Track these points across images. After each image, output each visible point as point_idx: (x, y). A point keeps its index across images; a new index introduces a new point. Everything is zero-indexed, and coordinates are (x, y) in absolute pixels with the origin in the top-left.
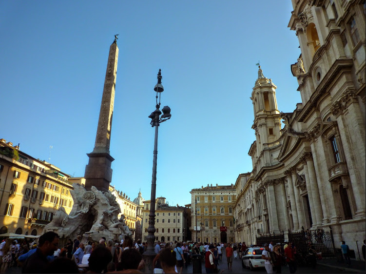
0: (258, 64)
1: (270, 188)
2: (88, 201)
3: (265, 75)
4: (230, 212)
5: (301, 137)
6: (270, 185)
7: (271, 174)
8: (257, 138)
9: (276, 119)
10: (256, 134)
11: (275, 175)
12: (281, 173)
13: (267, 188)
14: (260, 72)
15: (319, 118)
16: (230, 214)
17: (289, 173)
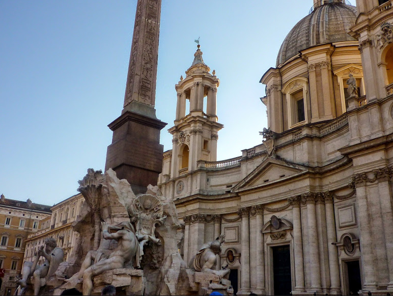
0: (197, 41)
1: (197, 227)
2: (144, 215)
3: (206, 60)
4: (18, 245)
5: (310, 171)
6: (200, 222)
7: (204, 206)
8: (176, 148)
9: (215, 130)
10: (175, 141)
11: (210, 209)
12: (223, 207)
13: (190, 225)
14: (198, 55)
15: (388, 160)
16: (17, 249)
17: (248, 212)
